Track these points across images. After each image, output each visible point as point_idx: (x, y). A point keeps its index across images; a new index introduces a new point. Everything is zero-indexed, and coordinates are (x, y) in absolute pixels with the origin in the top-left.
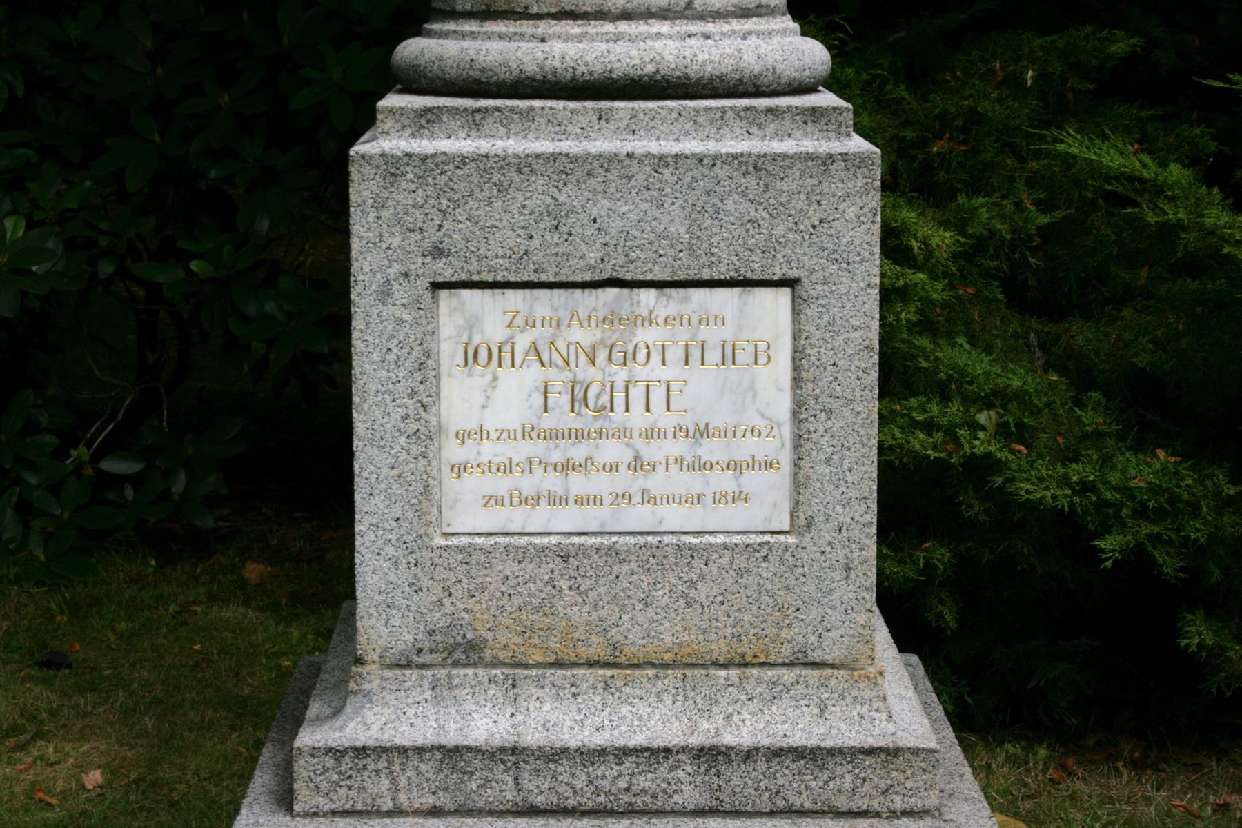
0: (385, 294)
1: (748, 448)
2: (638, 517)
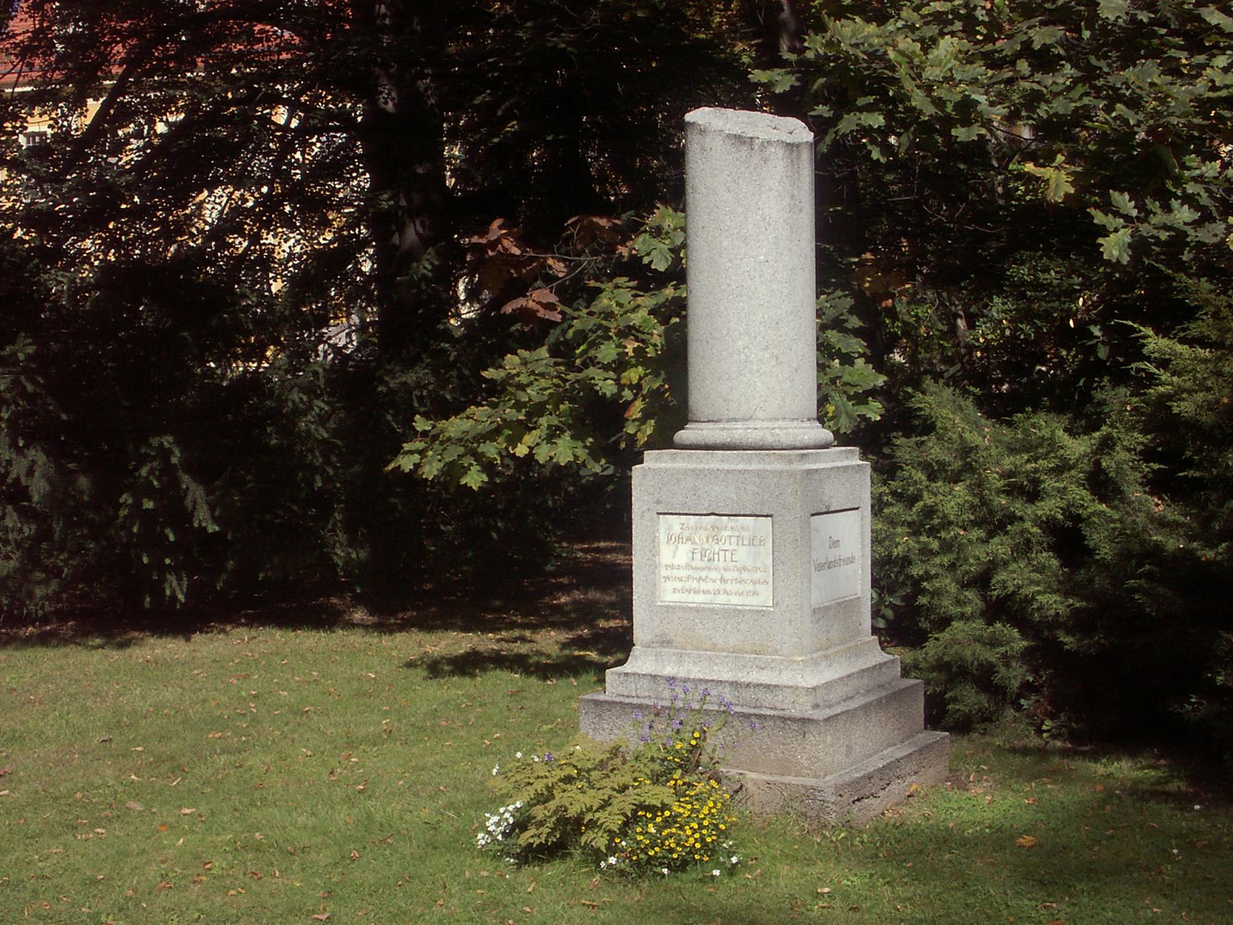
0: (642, 516)
1: (758, 575)
2: (722, 599)
